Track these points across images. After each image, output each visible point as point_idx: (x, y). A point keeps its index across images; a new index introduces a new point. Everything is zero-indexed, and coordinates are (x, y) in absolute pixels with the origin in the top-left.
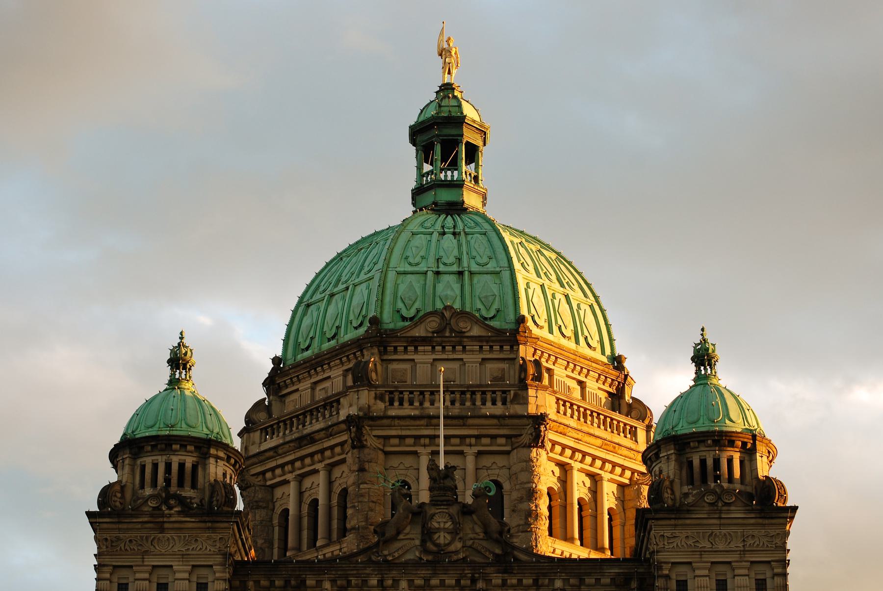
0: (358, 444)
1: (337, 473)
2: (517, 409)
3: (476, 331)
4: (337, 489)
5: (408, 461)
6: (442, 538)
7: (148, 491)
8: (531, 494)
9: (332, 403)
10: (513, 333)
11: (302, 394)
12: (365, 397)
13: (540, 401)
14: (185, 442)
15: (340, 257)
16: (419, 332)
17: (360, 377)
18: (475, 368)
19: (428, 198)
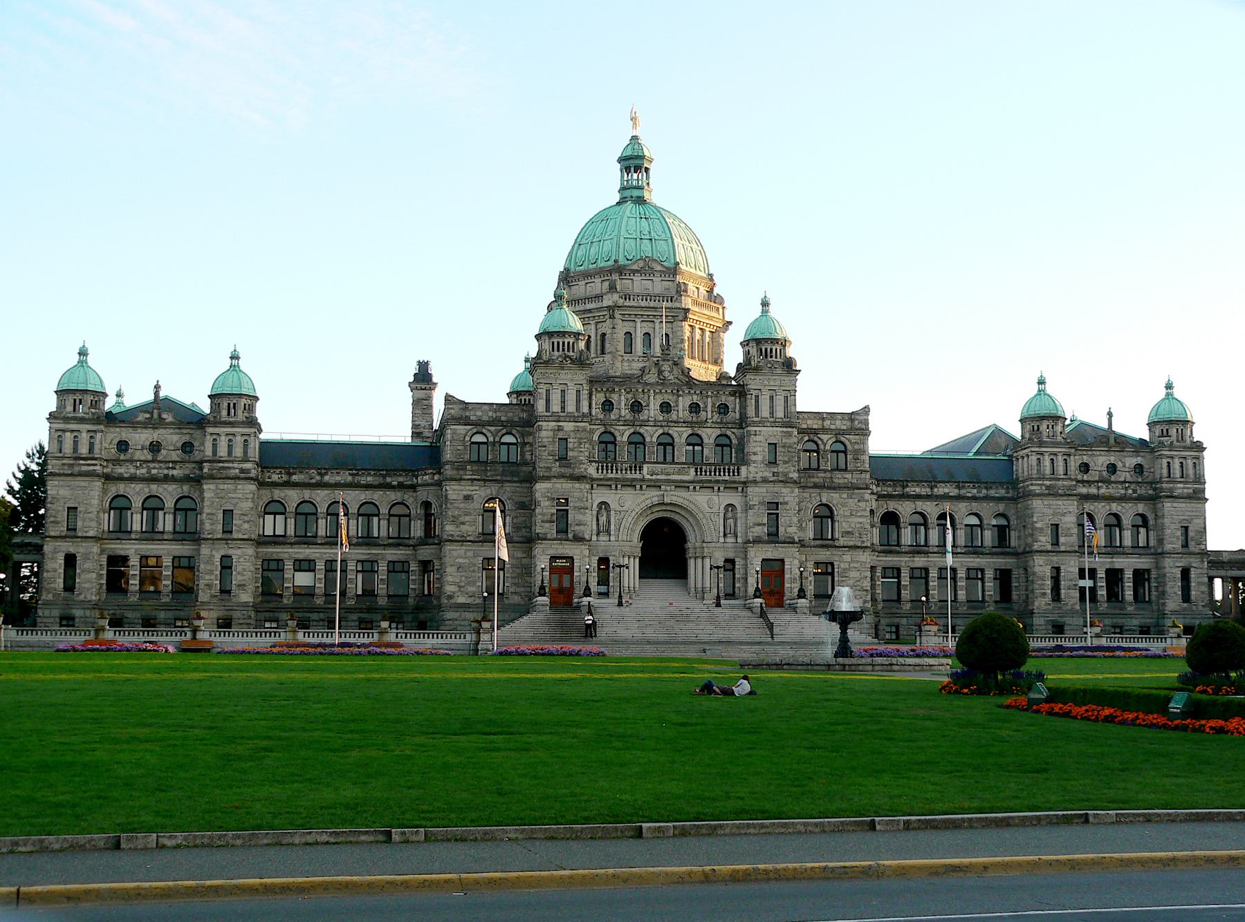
0: (612, 317)
1: (599, 326)
2: (677, 305)
3: (659, 268)
4: (600, 333)
5: (631, 324)
6: (666, 374)
7: (556, 353)
8: (682, 341)
9: (599, 297)
10: (674, 270)
11: (580, 289)
12: (616, 297)
13: (687, 302)
14: (570, 334)
15: (591, 221)
16: (635, 267)
17: (612, 288)
18: (658, 285)
19: (627, 193)
